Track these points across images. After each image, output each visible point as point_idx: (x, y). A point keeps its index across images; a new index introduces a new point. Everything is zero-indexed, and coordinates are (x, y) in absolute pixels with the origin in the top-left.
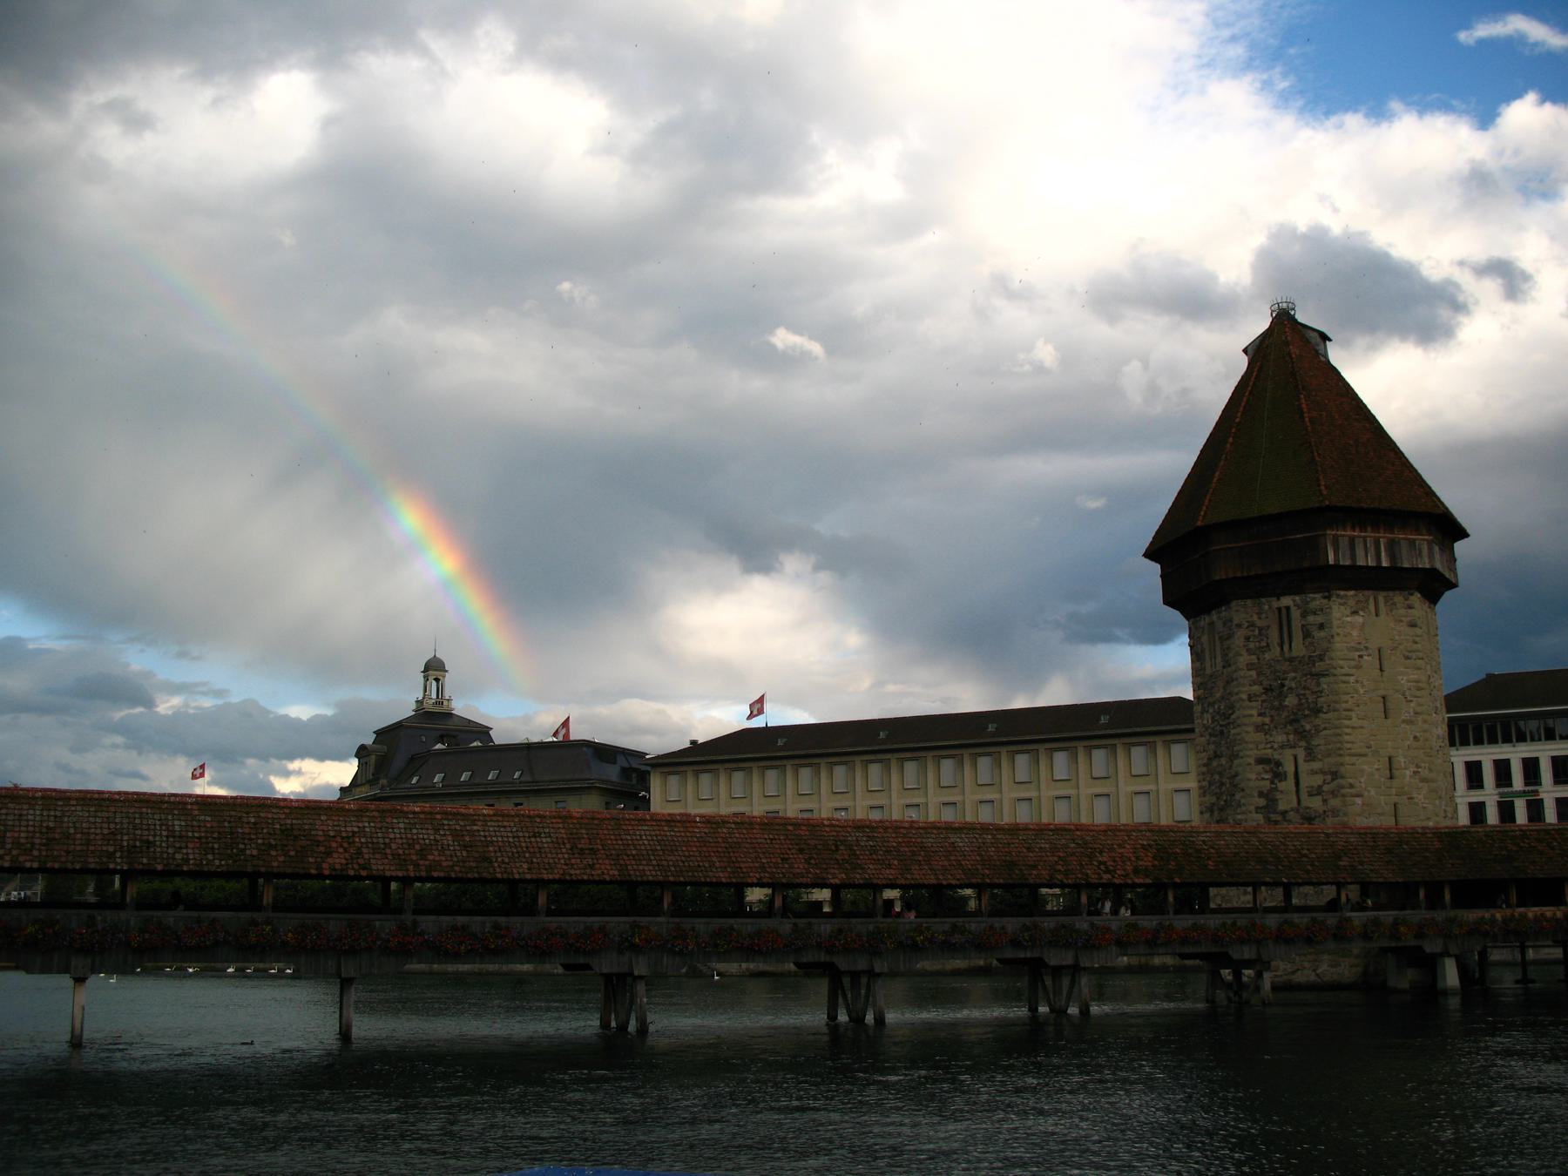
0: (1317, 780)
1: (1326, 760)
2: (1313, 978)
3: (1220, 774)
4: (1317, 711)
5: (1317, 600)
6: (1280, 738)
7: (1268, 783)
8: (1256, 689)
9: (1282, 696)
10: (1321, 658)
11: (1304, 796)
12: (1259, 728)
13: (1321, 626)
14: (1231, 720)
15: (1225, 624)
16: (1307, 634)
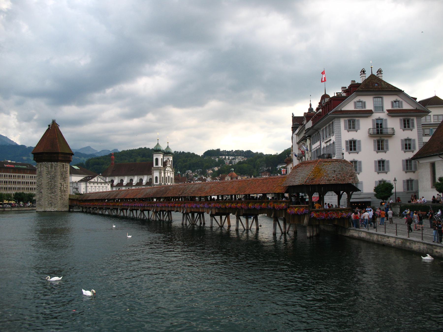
0: (66, 186)
1: (67, 184)
2: (64, 210)
3: (51, 184)
4: (66, 178)
5: (67, 164)
6: (62, 181)
7: (60, 186)
8: (60, 174)
9: (63, 175)
10: (67, 171)
11: (64, 188)
12: (60, 179)
13: (67, 167)
14: (56, 177)
15: (55, 165)
16: (66, 168)
